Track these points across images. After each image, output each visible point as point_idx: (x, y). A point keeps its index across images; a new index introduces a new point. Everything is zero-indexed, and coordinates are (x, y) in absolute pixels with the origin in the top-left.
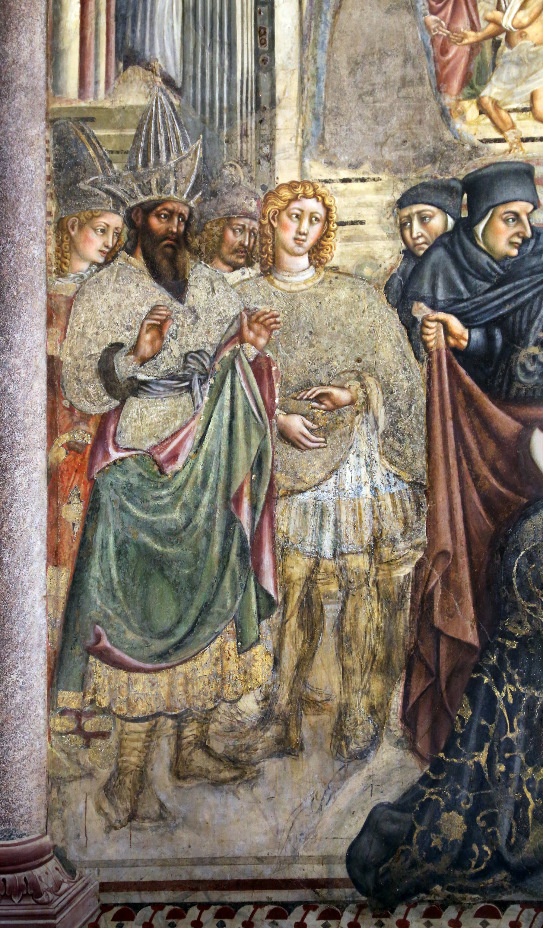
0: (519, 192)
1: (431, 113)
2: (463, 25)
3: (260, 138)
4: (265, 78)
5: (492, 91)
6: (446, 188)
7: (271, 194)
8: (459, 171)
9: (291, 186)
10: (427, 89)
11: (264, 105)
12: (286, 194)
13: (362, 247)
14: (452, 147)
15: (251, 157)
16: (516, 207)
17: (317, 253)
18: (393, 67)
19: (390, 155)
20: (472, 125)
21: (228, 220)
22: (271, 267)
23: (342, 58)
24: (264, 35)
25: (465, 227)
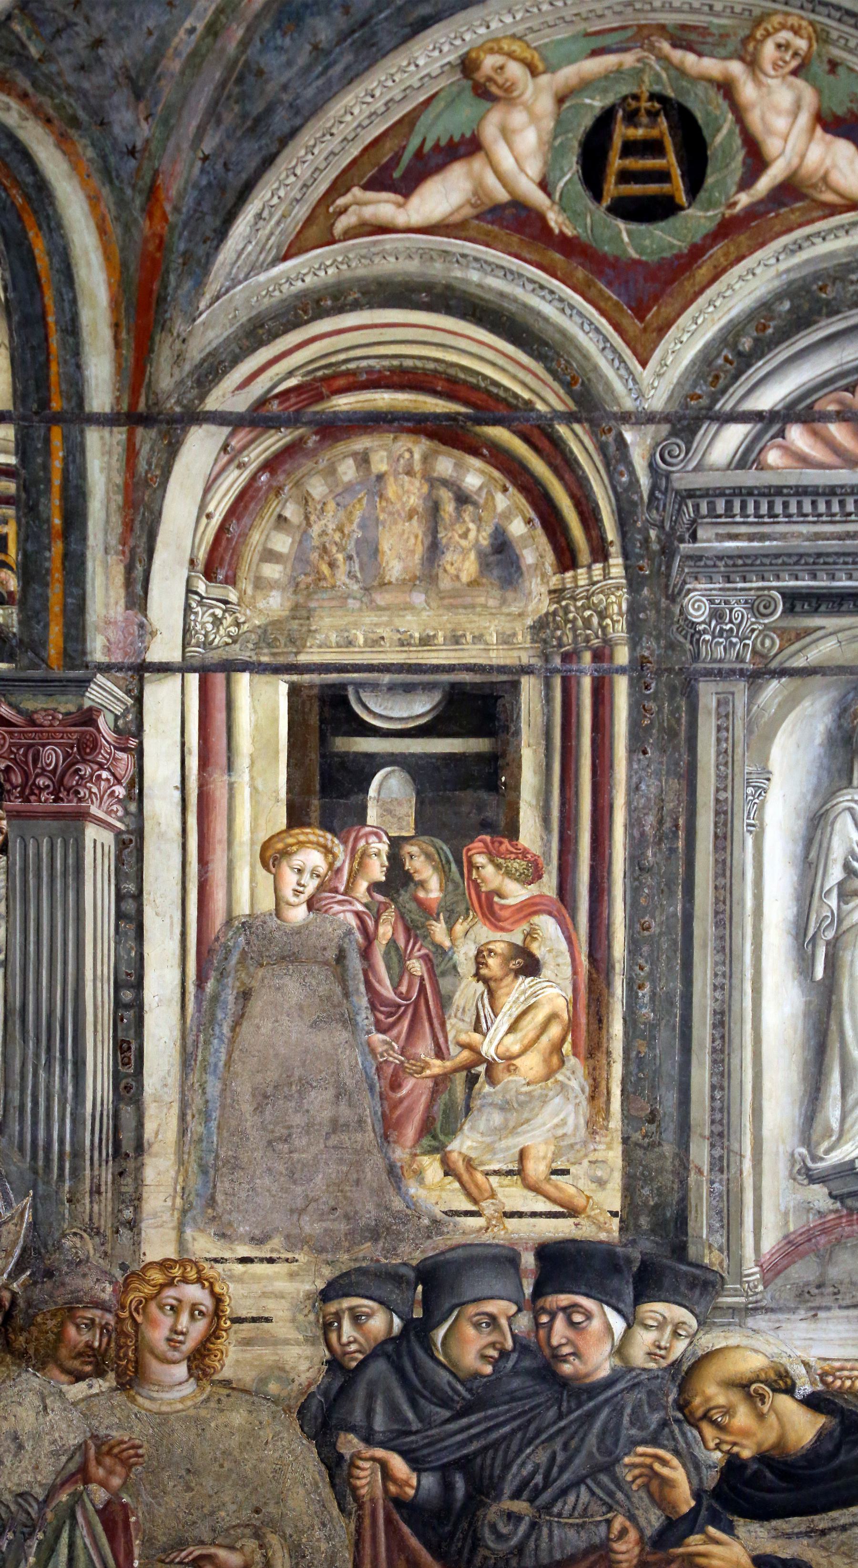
0: (498, 1287)
1: (373, 1169)
2: (424, 1049)
3: (118, 1195)
4: (127, 1112)
5: (463, 1144)
6: (394, 1277)
7: (133, 1277)
8: (412, 1254)
9: (164, 1265)
10: (368, 1137)
11: (126, 1150)
12: (157, 1276)
13: (267, 1354)
14: (404, 1219)
15: (105, 1224)
16: (491, 1307)
17: (200, 1360)
18: (320, 1102)
19: (311, 1226)
20: (433, 1189)
21: (69, 1311)
22: (132, 1377)
23: (243, 1088)
24: (128, 1051)
25: (418, 1332)
